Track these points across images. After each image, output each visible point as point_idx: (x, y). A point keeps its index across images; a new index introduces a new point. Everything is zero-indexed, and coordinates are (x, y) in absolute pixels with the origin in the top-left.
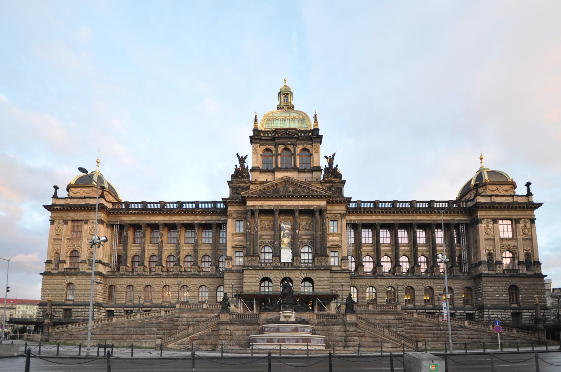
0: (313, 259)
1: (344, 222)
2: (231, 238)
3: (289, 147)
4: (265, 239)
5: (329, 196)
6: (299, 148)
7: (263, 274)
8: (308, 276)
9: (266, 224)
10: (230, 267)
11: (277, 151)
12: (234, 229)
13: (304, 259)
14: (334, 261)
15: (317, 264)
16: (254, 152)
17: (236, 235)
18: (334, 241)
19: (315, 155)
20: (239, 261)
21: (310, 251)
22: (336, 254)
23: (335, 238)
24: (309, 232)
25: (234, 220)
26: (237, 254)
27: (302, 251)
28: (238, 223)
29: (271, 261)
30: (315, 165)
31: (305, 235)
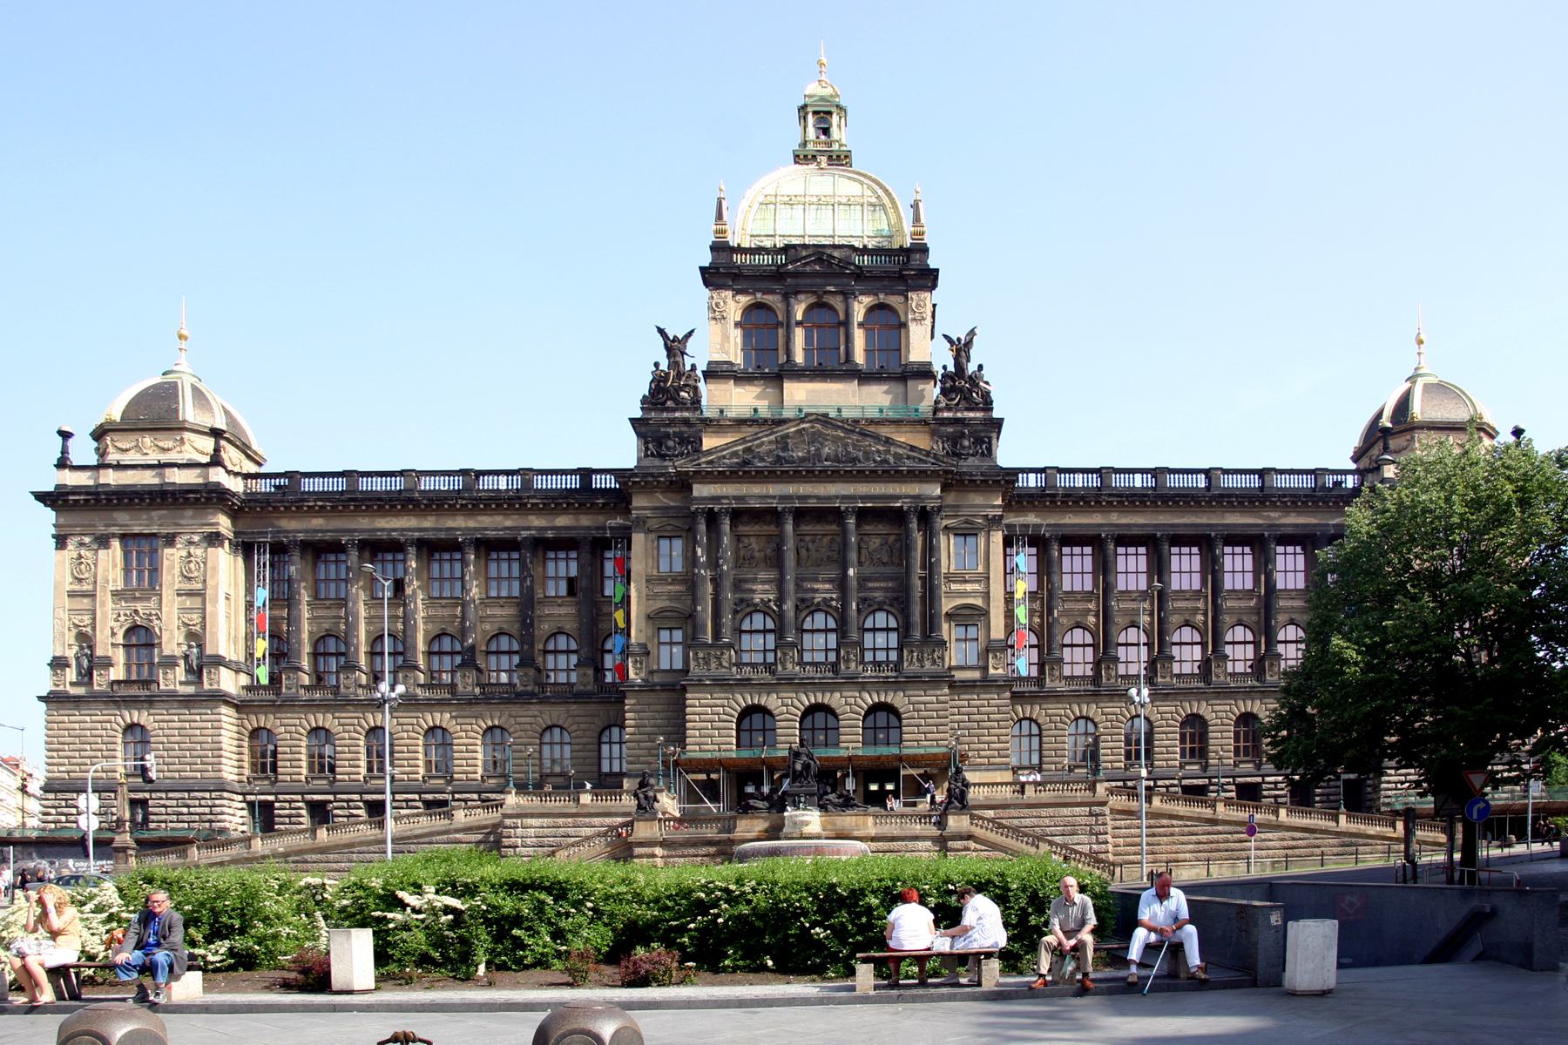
1: (997, 538)
2: (644, 591)
7: (743, 700)
9: (755, 546)
11: (789, 313)
12: (650, 561)
13: (874, 649)
16: (716, 314)
17: (662, 580)
18: (965, 594)
19: (913, 327)
20: (670, 657)
21: (893, 624)
23: (969, 587)
24: (888, 570)
26: (665, 636)
28: (664, 543)
29: (770, 658)
30: (912, 359)
31: (877, 580)
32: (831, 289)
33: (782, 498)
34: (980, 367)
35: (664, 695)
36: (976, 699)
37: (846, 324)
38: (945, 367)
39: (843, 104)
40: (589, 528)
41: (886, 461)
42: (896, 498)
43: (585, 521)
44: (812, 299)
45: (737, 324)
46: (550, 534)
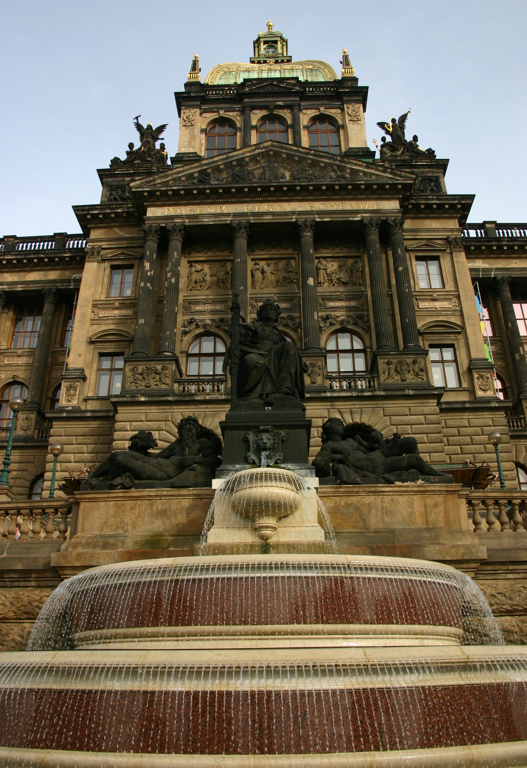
0: (372, 369)
2: (90, 315)
3: (275, 112)
4: (201, 312)
5: (407, 187)
6: (305, 118)
8: (357, 420)
10: (75, 402)
14: (442, 374)
15: (387, 377)
19: (350, 127)
22: (448, 355)
23: (438, 305)
25: (107, 265)
26: (106, 364)
27: (331, 346)
32: (278, 103)
33: (236, 215)
34: (415, 138)
35: (94, 424)
36: (465, 418)
37: (295, 126)
38: (383, 139)
39: (285, 36)
40: (54, 281)
41: (343, 177)
42: (358, 212)
43: (53, 275)
44: (264, 113)
45: (203, 131)
46: (19, 288)
